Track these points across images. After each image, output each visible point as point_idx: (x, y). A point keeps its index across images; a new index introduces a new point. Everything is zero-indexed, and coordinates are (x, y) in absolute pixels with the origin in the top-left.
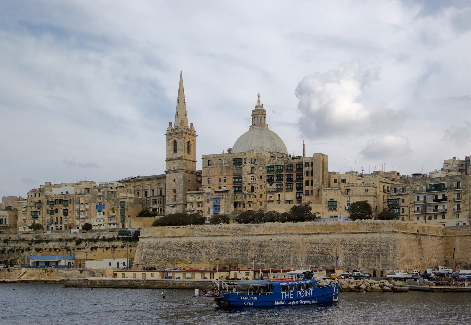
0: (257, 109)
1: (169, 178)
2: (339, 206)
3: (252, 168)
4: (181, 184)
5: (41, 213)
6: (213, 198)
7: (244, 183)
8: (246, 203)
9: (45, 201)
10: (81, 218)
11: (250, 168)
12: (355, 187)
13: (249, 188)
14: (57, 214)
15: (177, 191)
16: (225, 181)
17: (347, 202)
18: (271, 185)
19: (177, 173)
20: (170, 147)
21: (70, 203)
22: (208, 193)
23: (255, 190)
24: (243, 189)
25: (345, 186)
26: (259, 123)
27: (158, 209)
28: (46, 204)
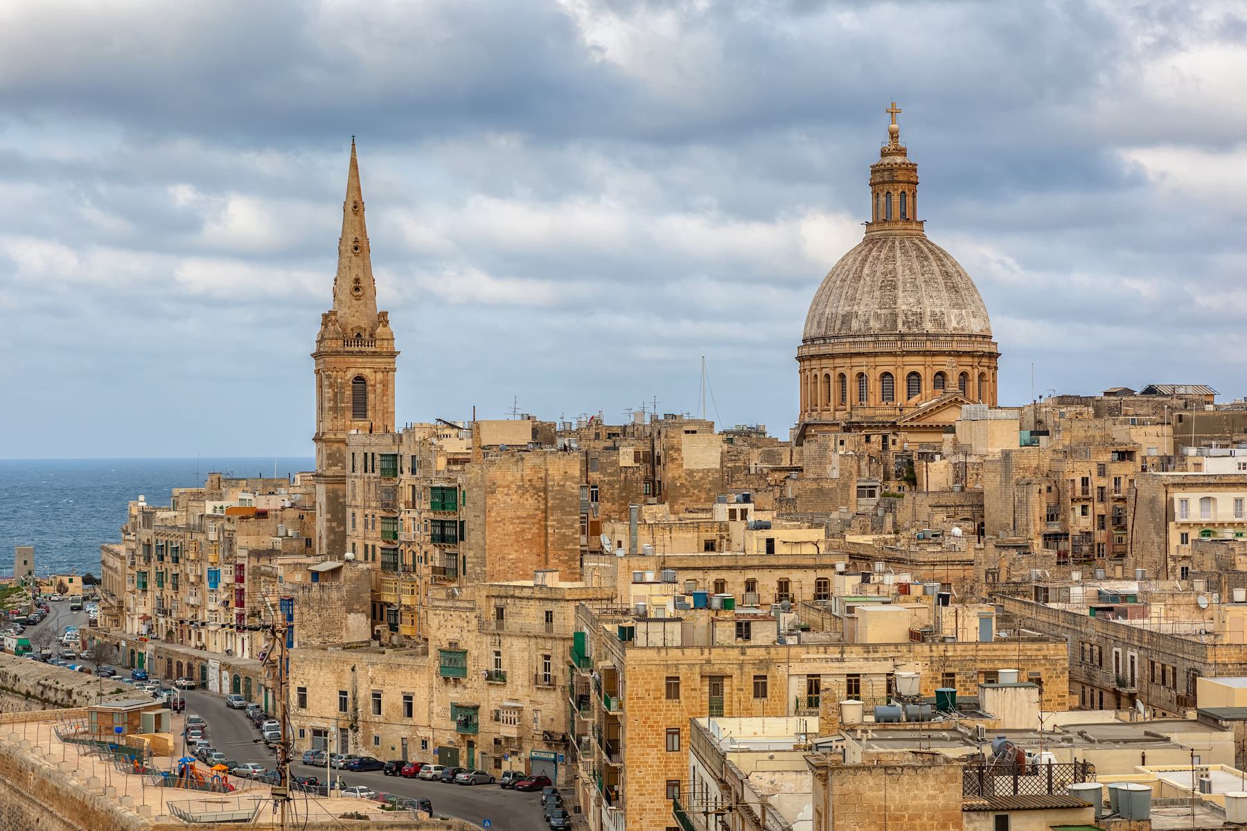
0: (887, 160)
2: (472, 668)
12: (517, 601)
17: (494, 657)
23: (418, 565)
25: (487, 596)
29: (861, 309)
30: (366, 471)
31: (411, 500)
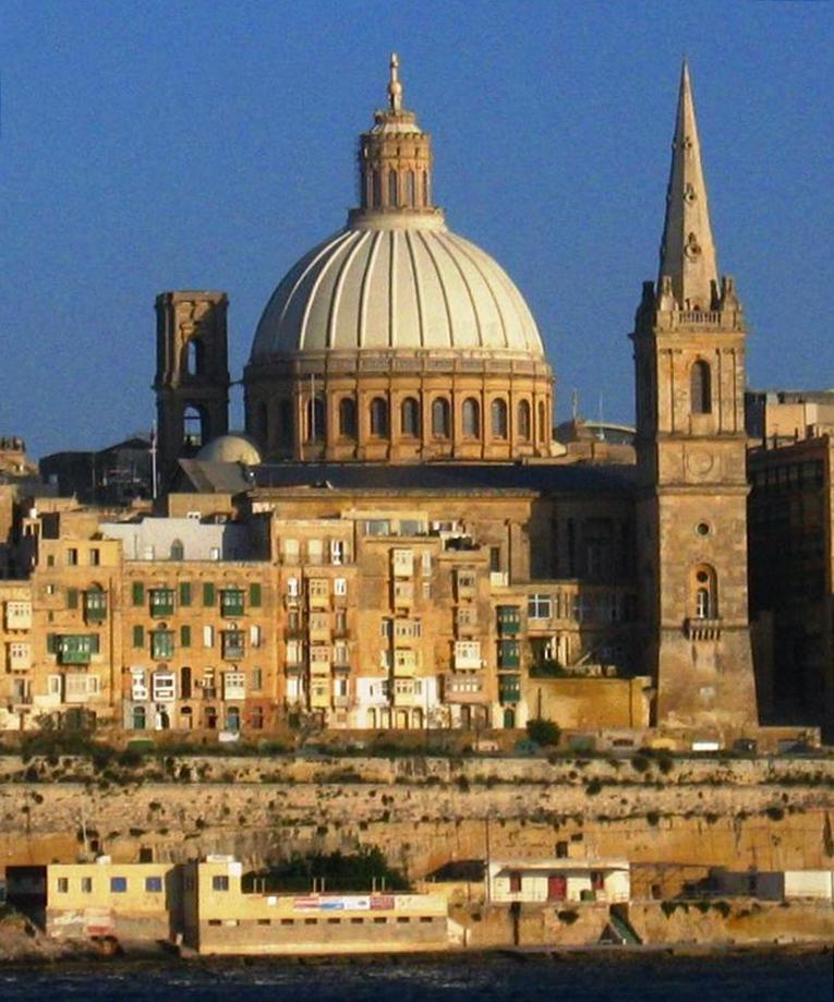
1: (675, 516)
5: (104, 643)
9: (123, 588)
10: (317, 675)
14: (188, 650)
15: (721, 573)
19: (718, 498)
21: (256, 602)
27: (554, 640)
28: (128, 600)
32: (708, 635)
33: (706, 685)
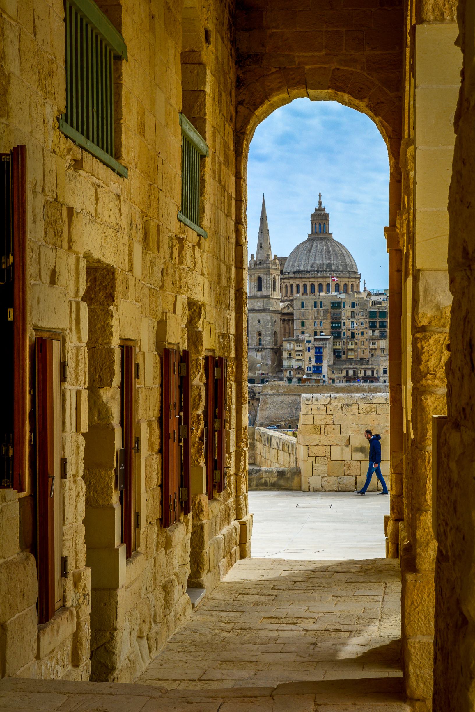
1: (252, 318)
3: (352, 312)
4: (268, 327)
6: (316, 347)
7: (344, 329)
8: (345, 350)
11: (350, 313)
13: (349, 334)
16: (321, 325)
18: (373, 331)
20: (253, 283)
22: (309, 341)
23: (356, 337)
24: (342, 335)
26: (322, 231)
29: (335, 262)
30: (315, 307)
31: (350, 315)
32: (260, 350)
33: (259, 364)
